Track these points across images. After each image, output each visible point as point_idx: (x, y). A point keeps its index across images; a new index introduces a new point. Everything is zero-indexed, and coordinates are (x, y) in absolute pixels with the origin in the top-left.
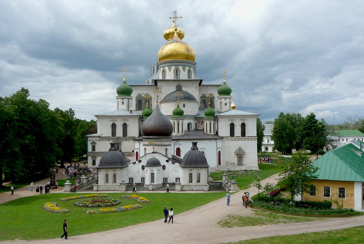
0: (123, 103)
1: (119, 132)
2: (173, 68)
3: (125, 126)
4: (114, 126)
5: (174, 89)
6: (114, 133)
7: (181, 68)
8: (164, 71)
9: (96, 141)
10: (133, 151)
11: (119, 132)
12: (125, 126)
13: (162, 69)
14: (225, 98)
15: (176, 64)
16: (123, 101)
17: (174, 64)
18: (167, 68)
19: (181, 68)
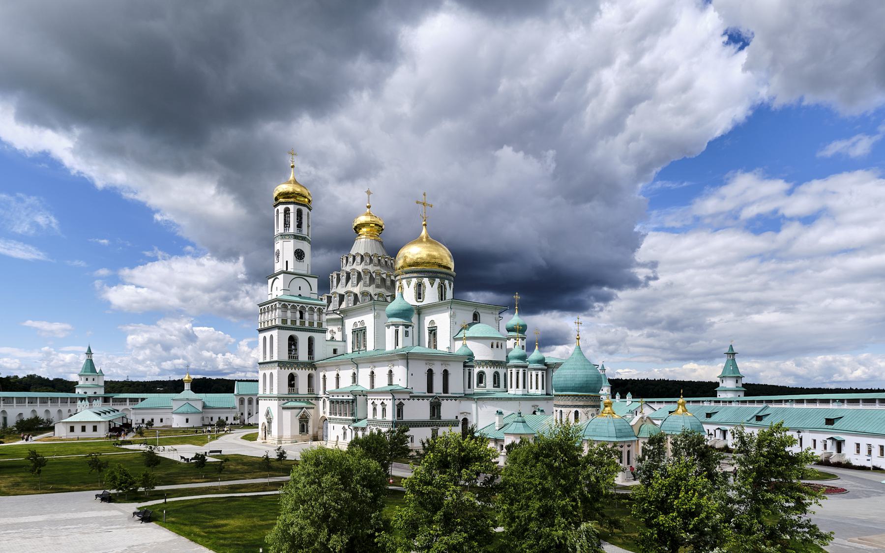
0: (407, 334)
1: (438, 387)
2: (438, 281)
3: (446, 374)
4: (430, 373)
5: (470, 319)
6: (430, 388)
7: (447, 282)
8: (419, 285)
9: (404, 399)
10: (457, 417)
11: (438, 387)
12: (446, 374)
13: (414, 281)
14: (523, 338)
15: (442, 275)
16: (407, 330)
17: (439, 275)
18: (426, 281)
19: (447, 282)
